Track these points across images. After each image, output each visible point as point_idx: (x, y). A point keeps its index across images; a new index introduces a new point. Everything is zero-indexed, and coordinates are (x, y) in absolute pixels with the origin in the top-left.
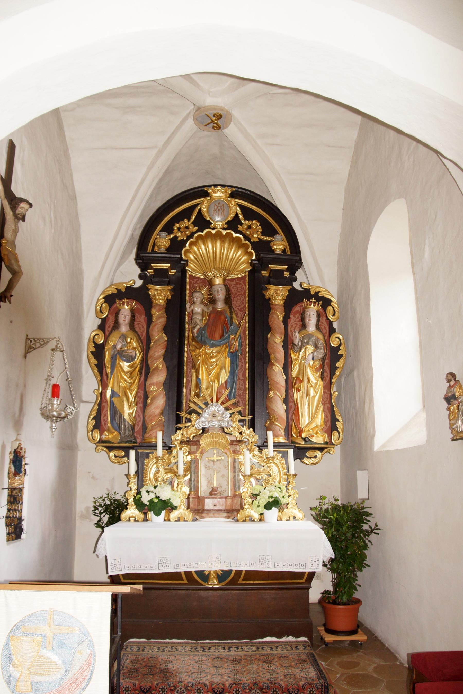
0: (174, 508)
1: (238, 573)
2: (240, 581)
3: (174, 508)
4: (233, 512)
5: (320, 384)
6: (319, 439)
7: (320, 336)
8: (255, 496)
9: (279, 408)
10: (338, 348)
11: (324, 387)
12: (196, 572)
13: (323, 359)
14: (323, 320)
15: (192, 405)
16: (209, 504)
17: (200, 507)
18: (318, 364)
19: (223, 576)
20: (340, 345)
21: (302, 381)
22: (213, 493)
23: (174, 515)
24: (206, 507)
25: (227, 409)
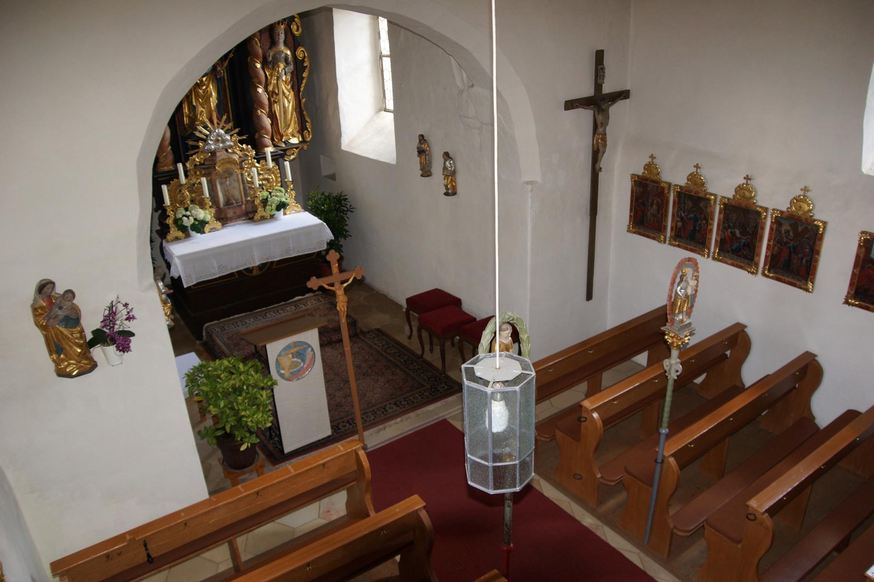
0: (207, 223)
1: (272, 262)
2: (274, 267)
3: (207, 223)
4: (250, 215)
5: (291, 96)
6: (295, 141)
7: (289, 53)
8: (265, 202)
9: (267, 122)
10: (303, 61)
11: (295, 95)
12: (245, 270)
13: (292, 73)
14: (289, 33)
15: (197, 134)
16: (230, 213)
17: (223, 216)
18: (289, 77)
19: (263, 265)
20: (305, 57)
21: (277, 95)
22: (228, 203)
23: (207, 228)
24: (229, 216)
25: (227, 132)
